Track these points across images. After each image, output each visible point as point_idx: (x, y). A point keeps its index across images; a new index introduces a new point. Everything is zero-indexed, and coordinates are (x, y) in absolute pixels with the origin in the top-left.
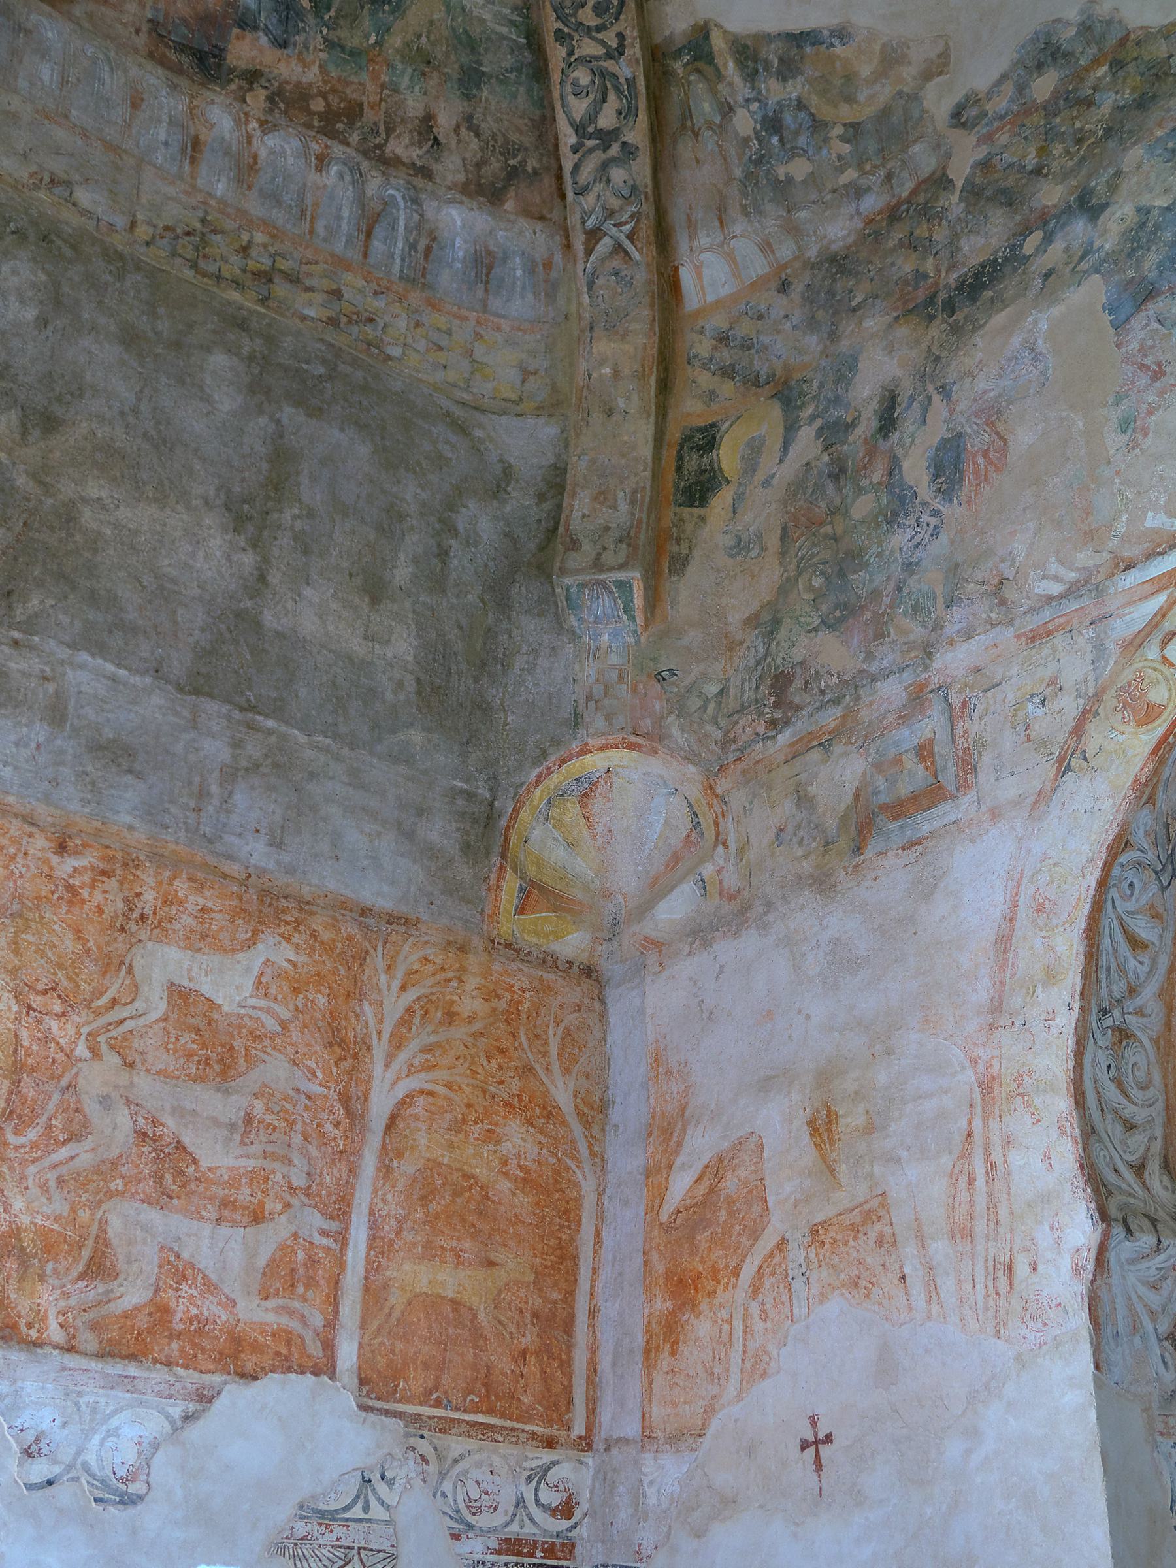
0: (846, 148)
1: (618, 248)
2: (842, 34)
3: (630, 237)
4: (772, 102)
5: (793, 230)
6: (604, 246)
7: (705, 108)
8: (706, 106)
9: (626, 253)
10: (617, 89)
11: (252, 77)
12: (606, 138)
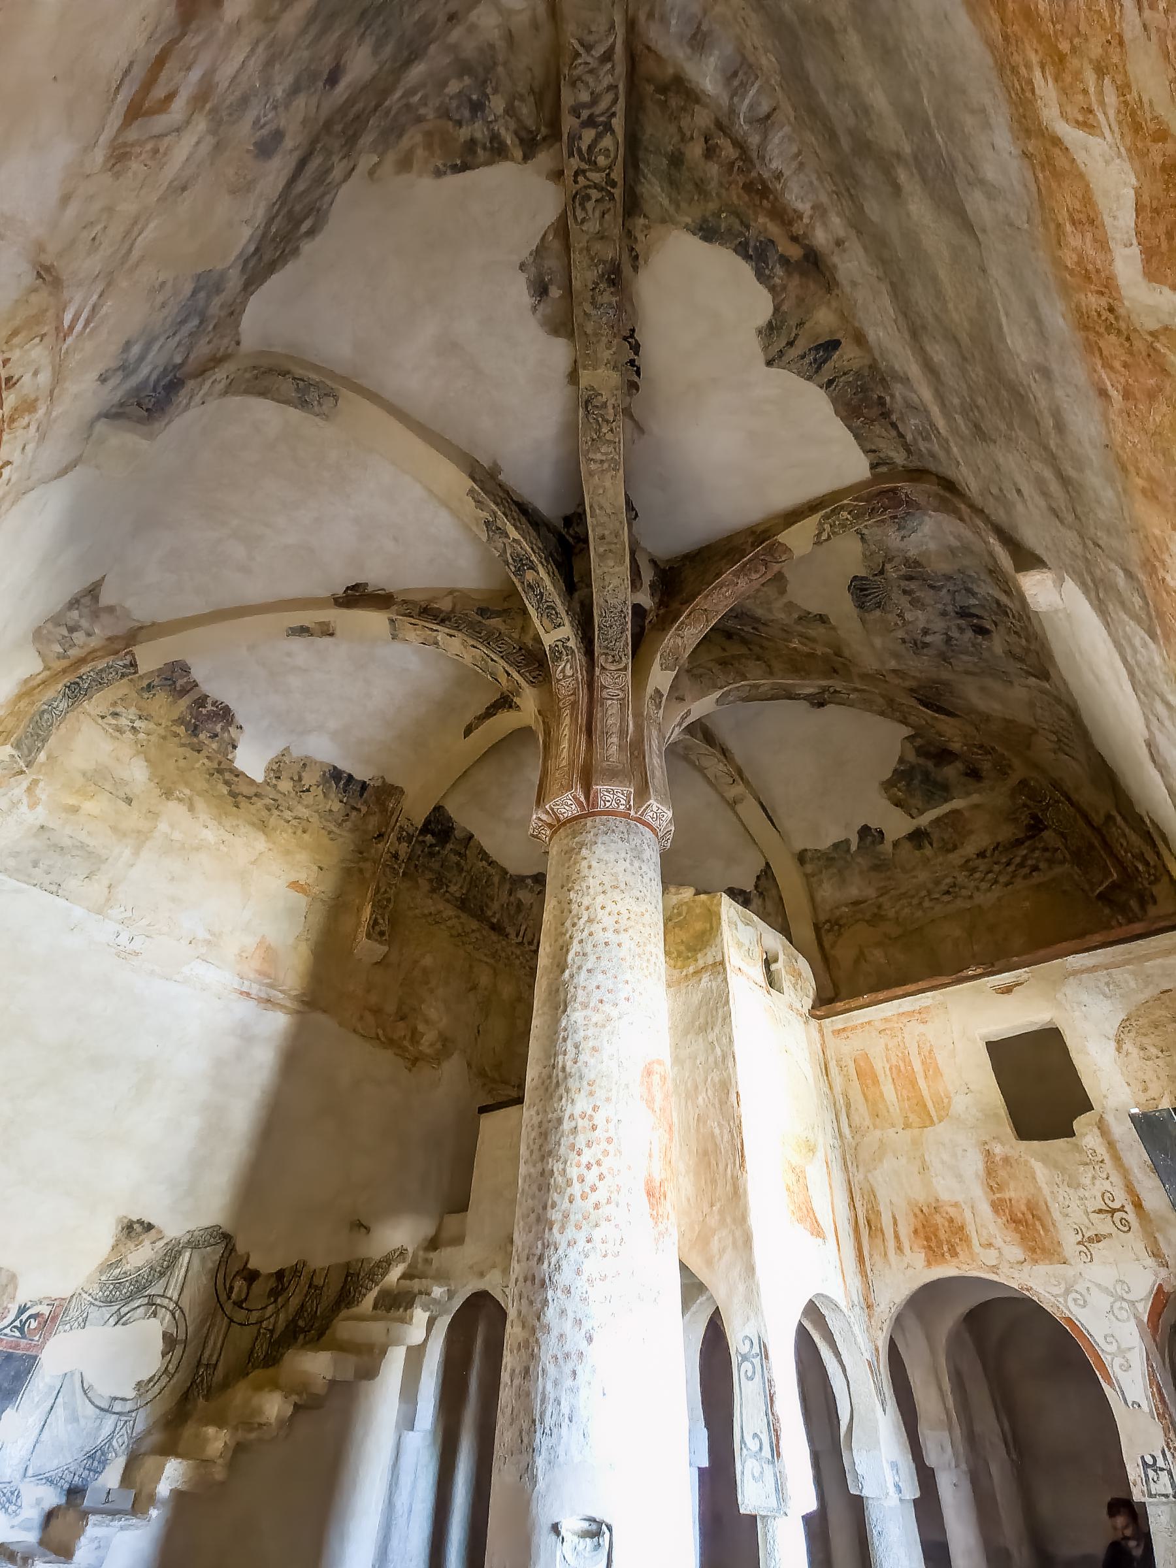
0: (422, 111)
1: (588, 48)
2: (439, 173)
3: (578, 55)
4: (478, 124)
5: (454, 48)
6: (599, 50)
7: (526, 110)
8: (525, 111)
9: (582, 45)
10: (580, 150)
11: (795, 239)
12: (590, 122)
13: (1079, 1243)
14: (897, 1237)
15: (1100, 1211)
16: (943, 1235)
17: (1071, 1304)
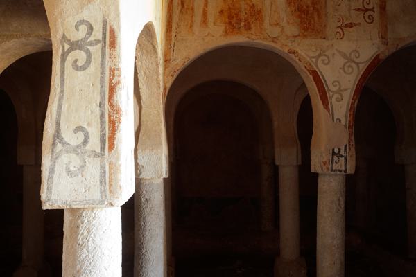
13: (338, 27)
14: (205, 14)
15: (358, 10)
16: (243, 15)
17: (320, 63)
